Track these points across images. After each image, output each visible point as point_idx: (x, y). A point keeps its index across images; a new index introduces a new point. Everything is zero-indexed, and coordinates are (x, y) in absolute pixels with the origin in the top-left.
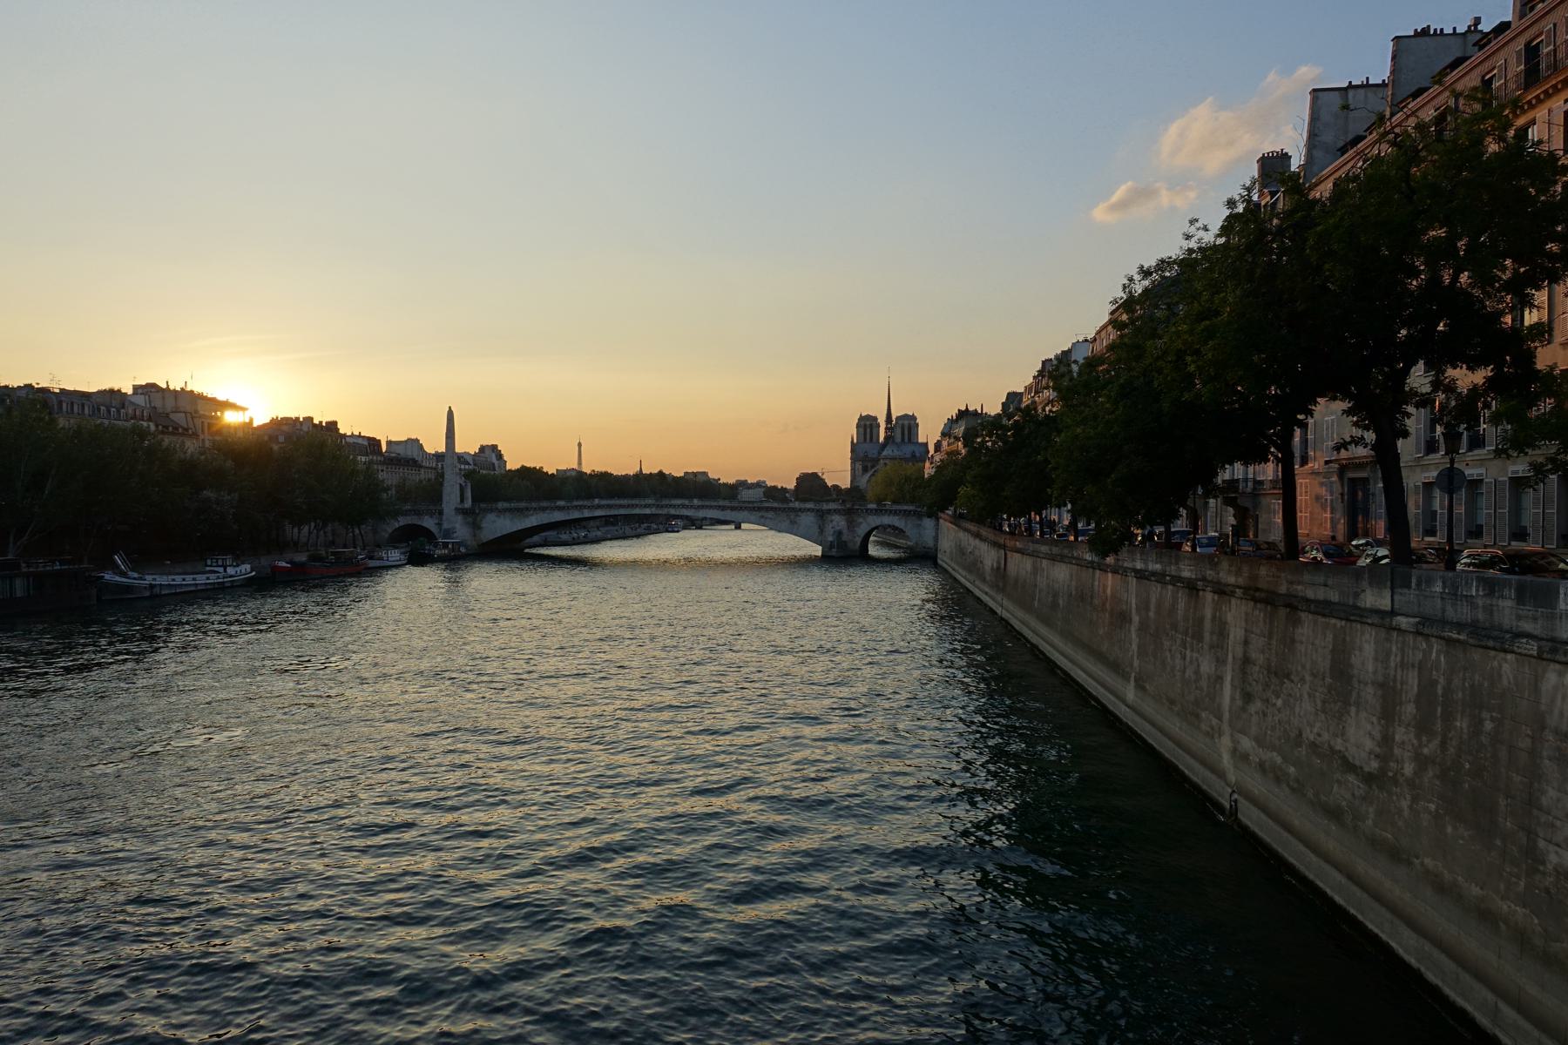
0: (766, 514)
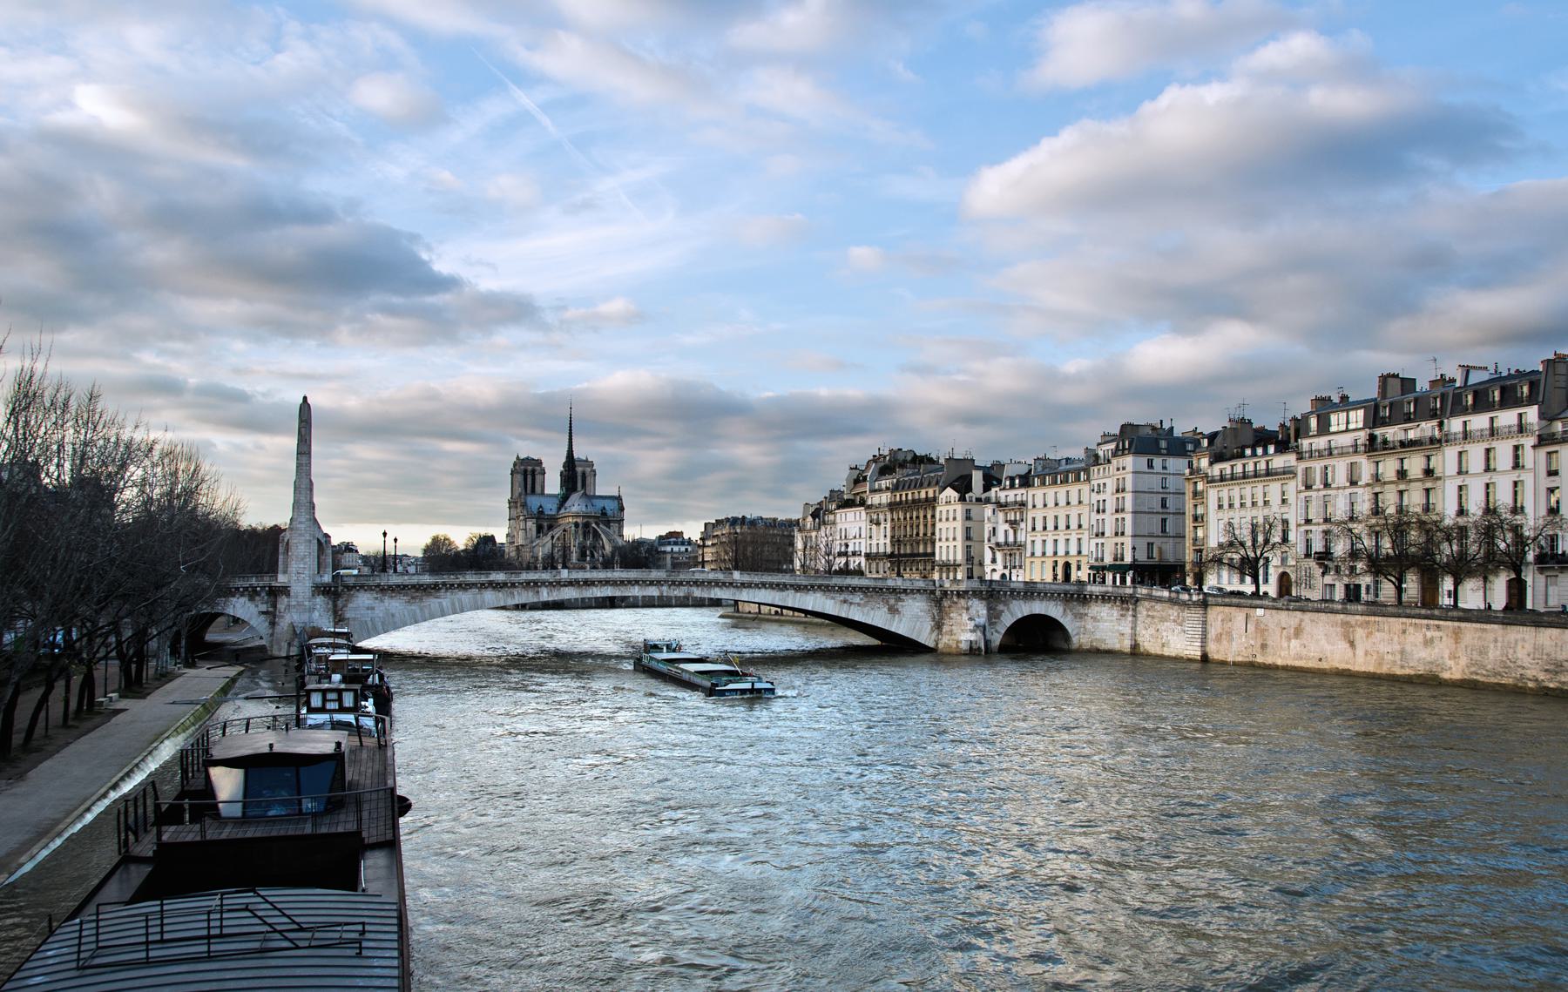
0: (850, 597)
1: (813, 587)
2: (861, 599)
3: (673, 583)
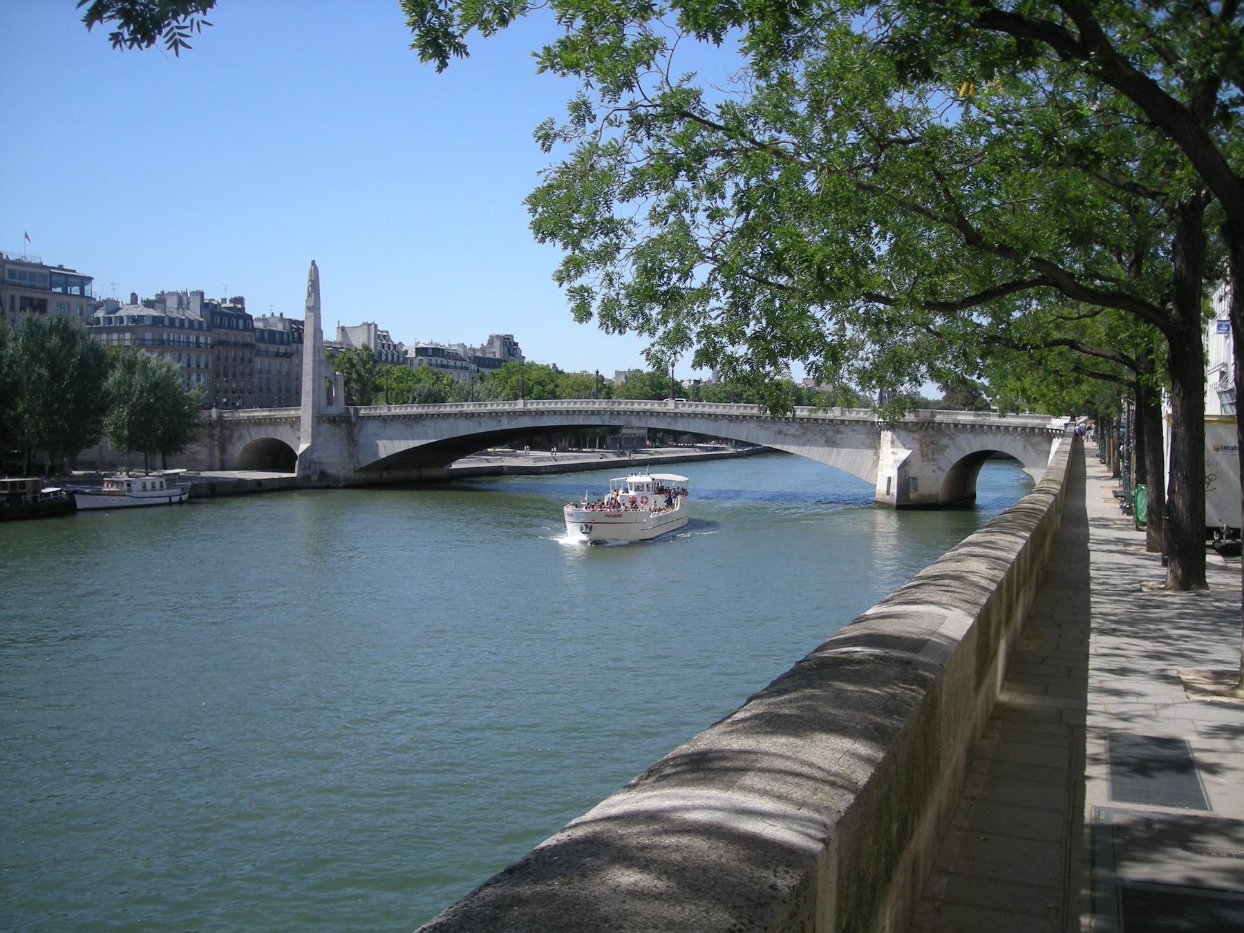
1: (744, 417)
2: (797, 430)
3: (612, 412)
